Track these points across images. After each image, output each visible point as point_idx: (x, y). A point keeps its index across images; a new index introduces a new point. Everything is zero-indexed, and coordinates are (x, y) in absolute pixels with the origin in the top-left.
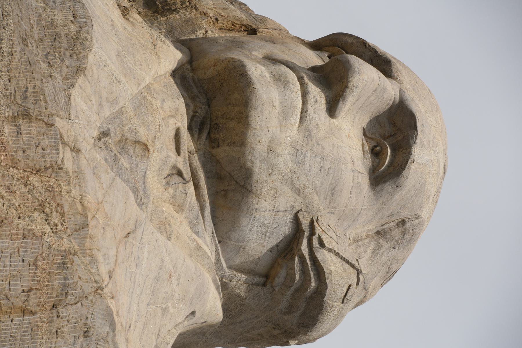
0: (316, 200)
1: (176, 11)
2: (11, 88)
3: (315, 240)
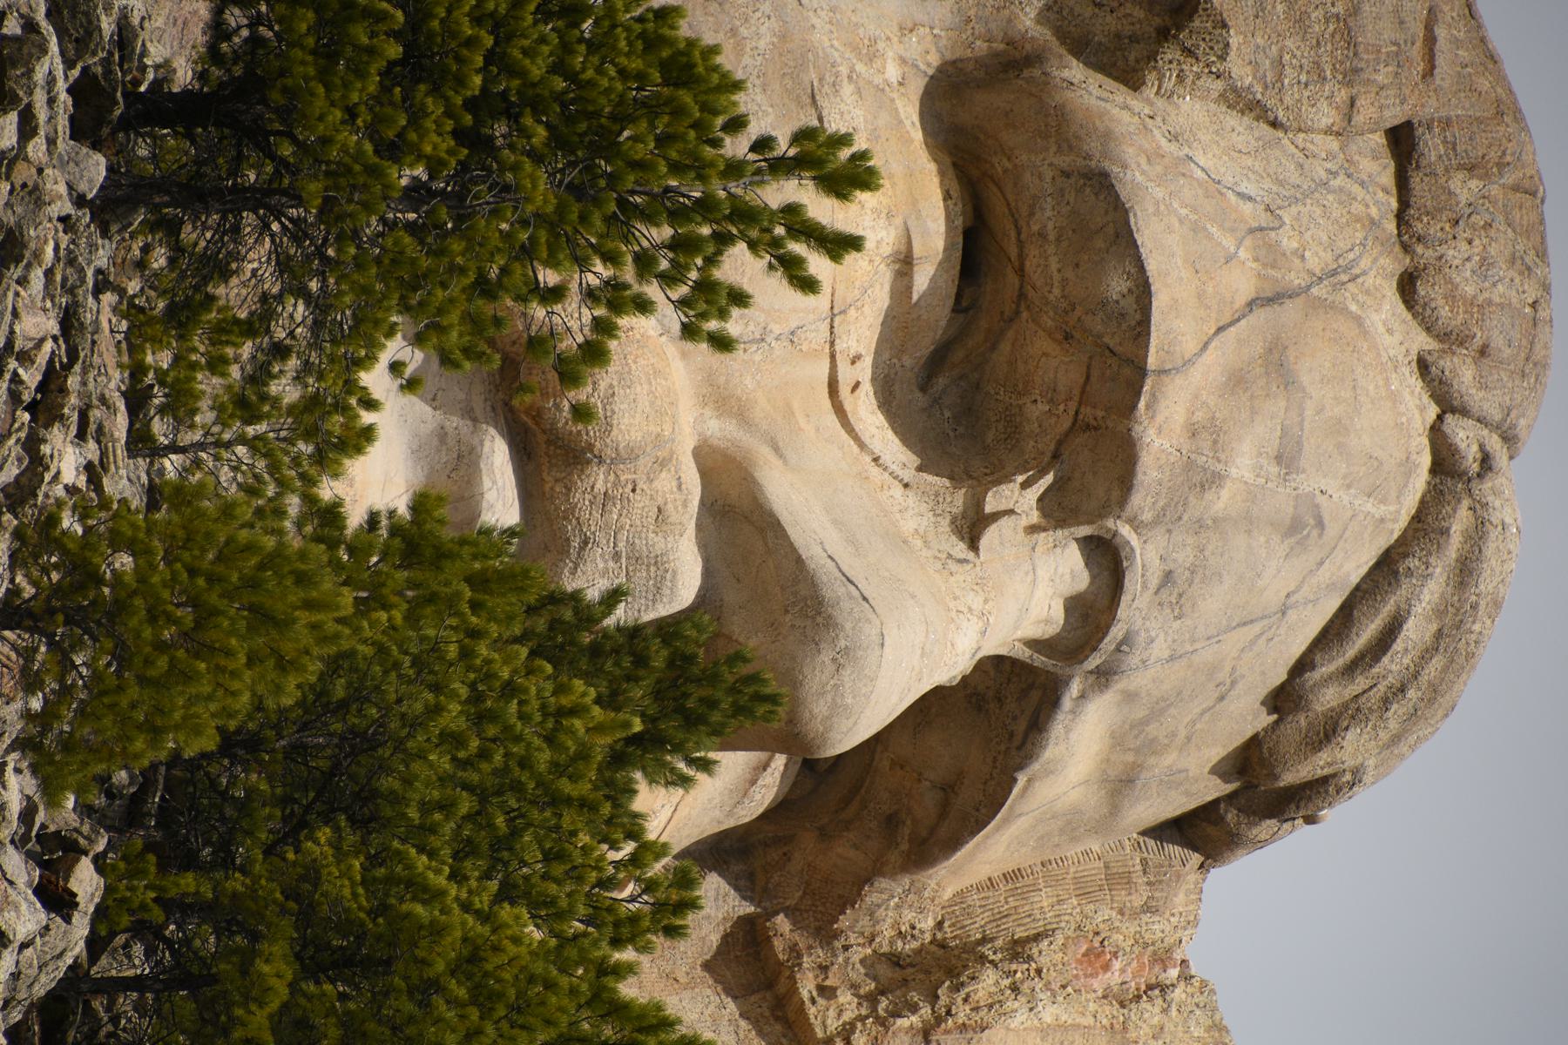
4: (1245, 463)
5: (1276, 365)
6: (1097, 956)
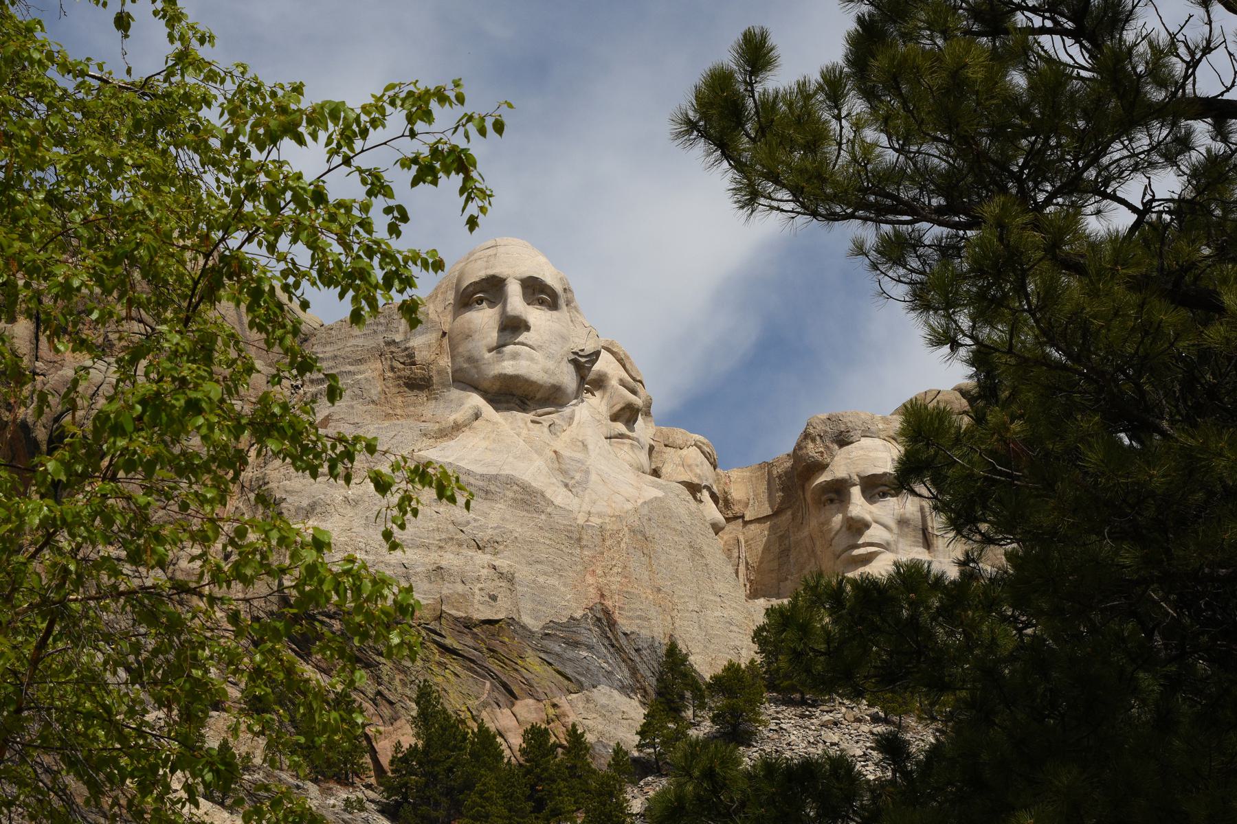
1: (431, 377)
4: (698, 471)
5: (689, 466)
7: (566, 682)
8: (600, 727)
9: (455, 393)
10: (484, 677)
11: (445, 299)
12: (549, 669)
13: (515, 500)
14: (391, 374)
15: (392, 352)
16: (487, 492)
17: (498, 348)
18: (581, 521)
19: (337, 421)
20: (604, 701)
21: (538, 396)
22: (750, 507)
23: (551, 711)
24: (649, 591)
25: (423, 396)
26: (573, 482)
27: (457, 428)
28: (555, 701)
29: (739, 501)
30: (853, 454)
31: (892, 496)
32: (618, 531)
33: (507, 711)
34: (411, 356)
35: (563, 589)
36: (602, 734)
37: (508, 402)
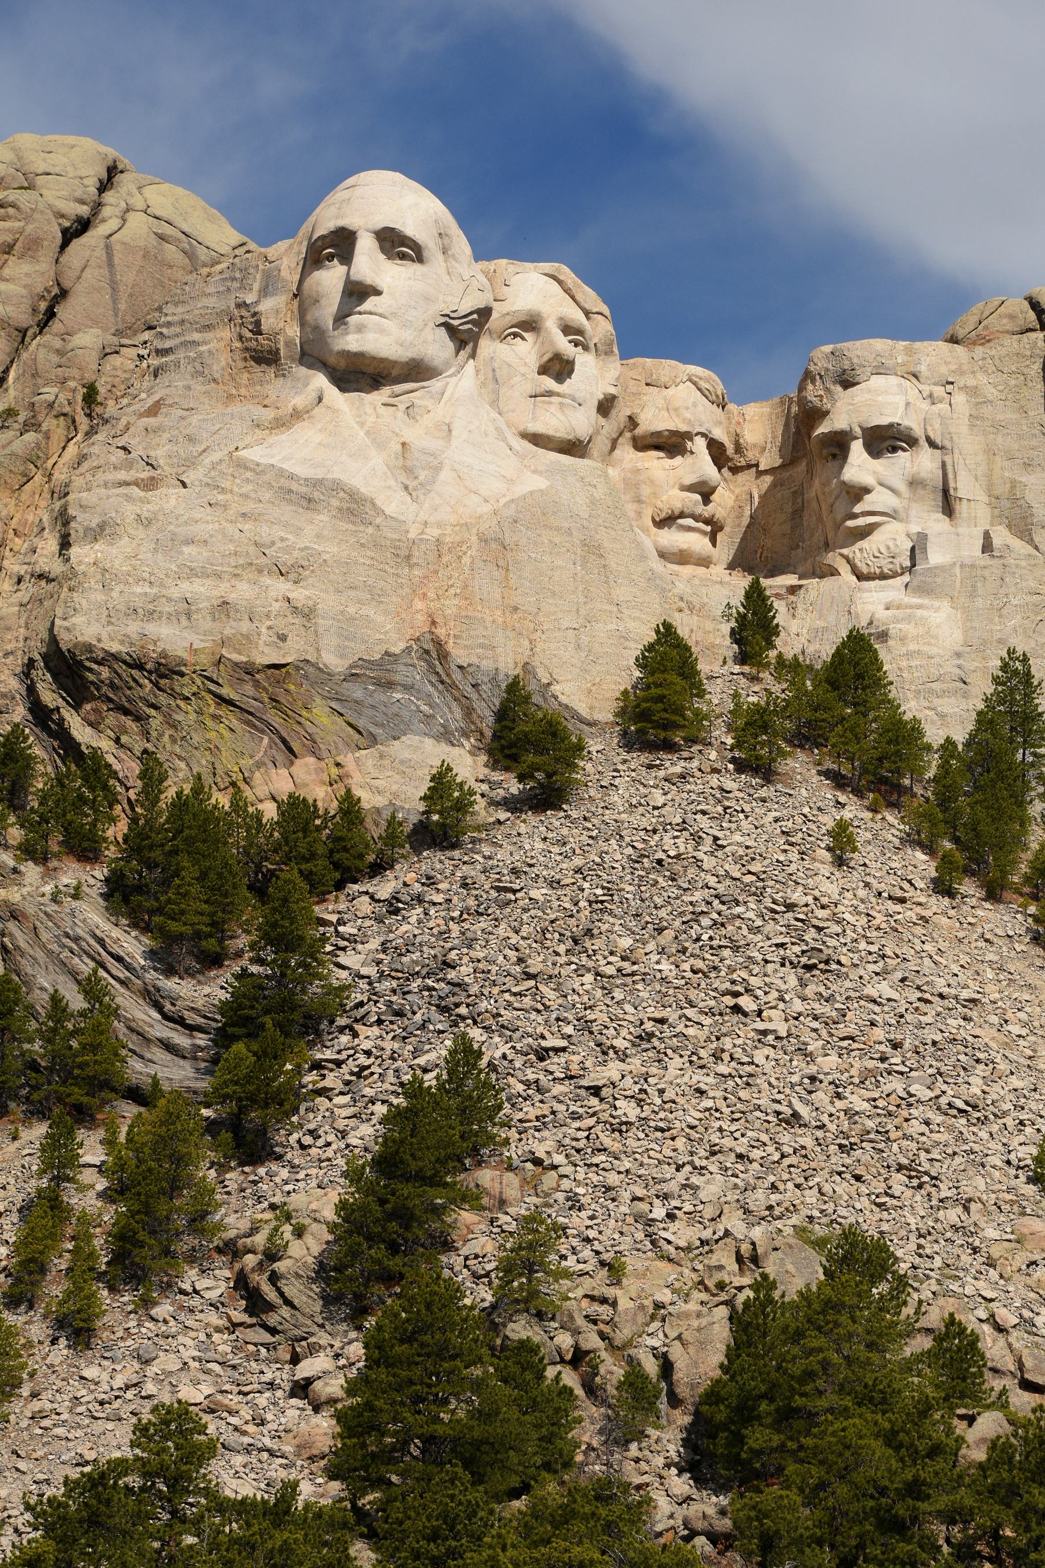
0: (430, 312)
1: (278, 349)
2: (393, 564)
3: (452, 315)
4: (688, 415)
5: (676, 410)
6: (739, 423)
7: (357, 736)
8: (395, 788)
9: (303, 371)
10: (262, 732)
11: (299, 253)
12: (339, 720)
13: (340, 510)
14: (238, 345)
15: (242, 317)
16: (310, 500)
17: (341, 318)
18: (412, 535)
19: (171, 406)
20: (406, 755)
21: (395, 372)
22: (767, 454)
23: (334, 771)
24: (499, 613)
25: (271, 371)
26: (416, 483)
27: (297, 415)
28: (339, 759)
29: (755, 445)
30: (857, 399)
31: (904, 450)
32: (460, 544)
33: (284, 772)
34: (258, 323)
35: (380, 619)
36: (396, 795)
37: (357, 382)
